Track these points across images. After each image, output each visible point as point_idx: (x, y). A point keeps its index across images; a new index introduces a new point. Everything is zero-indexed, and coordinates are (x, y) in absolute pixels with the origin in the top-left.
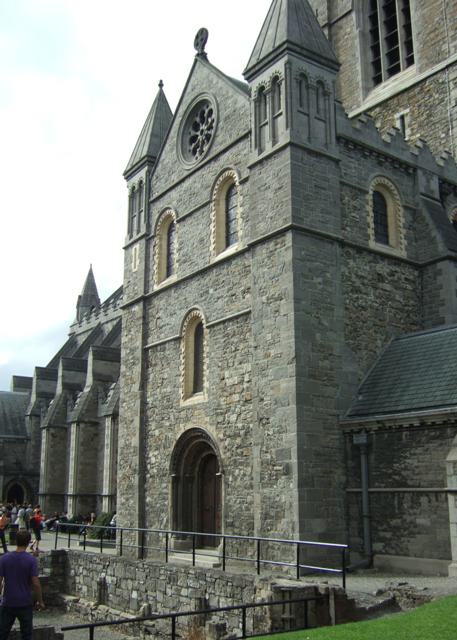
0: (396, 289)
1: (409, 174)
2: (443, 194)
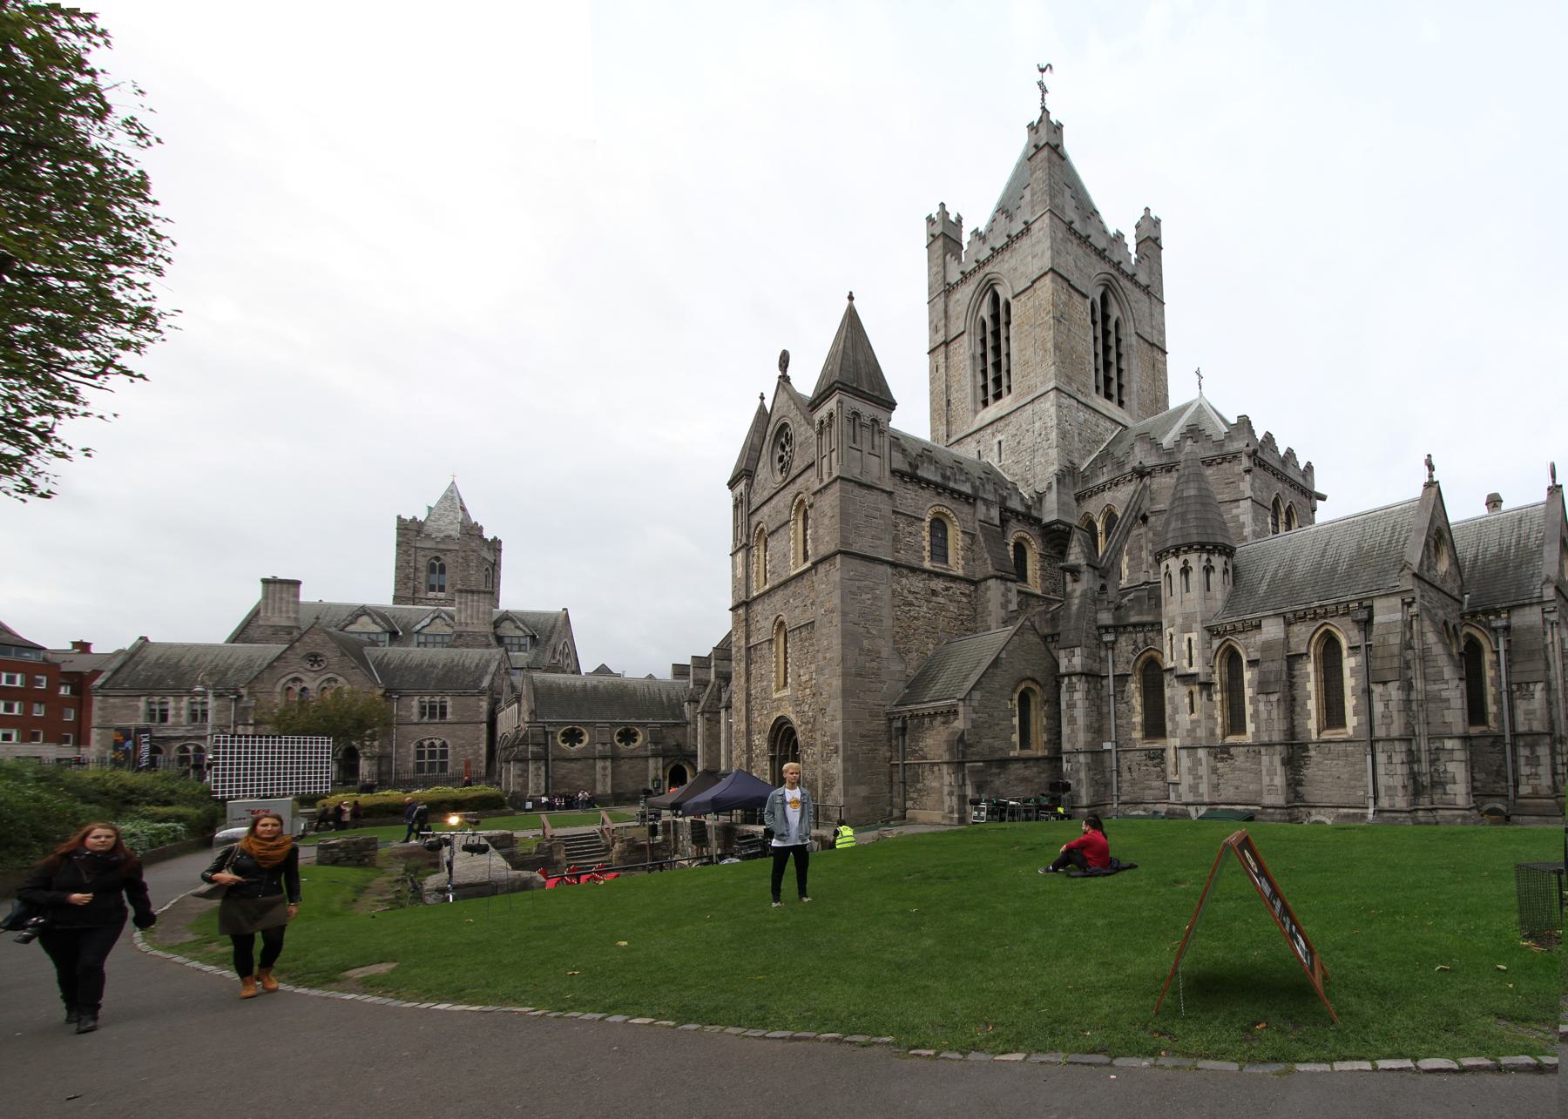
1: (969, 504)
2: (1004, 521)
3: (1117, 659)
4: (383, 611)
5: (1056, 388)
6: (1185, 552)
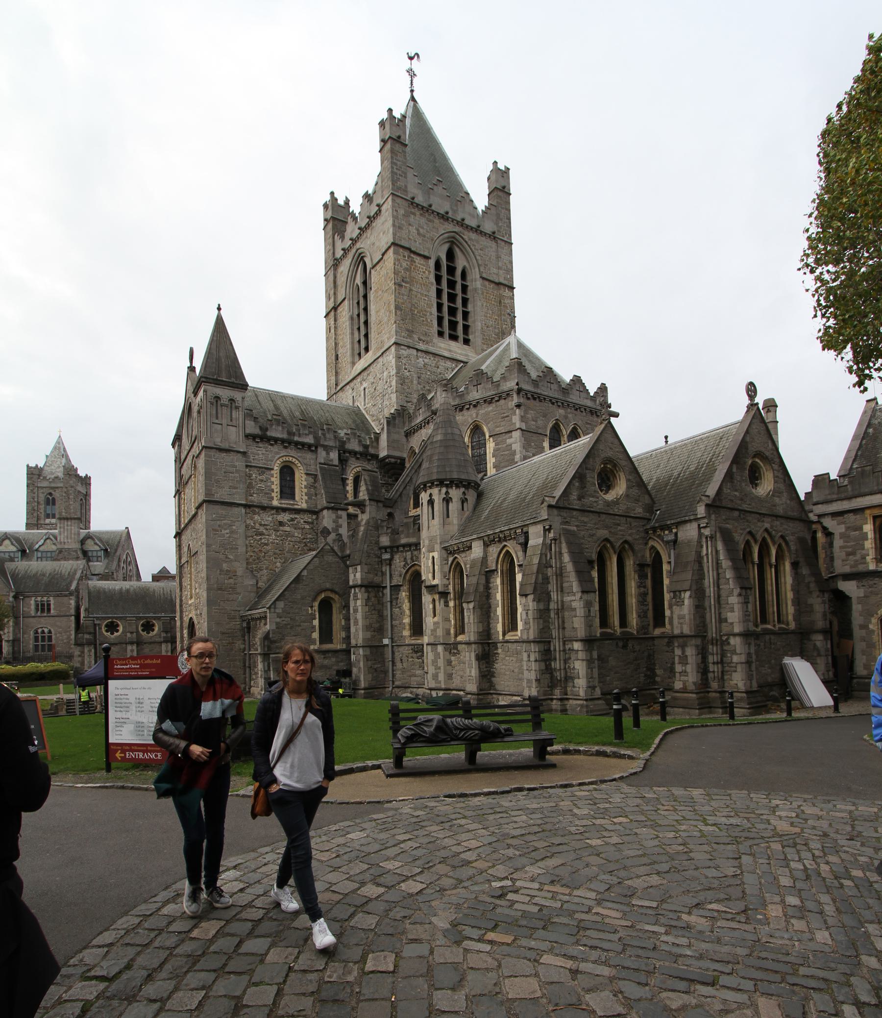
1: (312, 451)
2: (343, 461)
3: (393, 573)
5: (395, 343)
6: (430, 487)
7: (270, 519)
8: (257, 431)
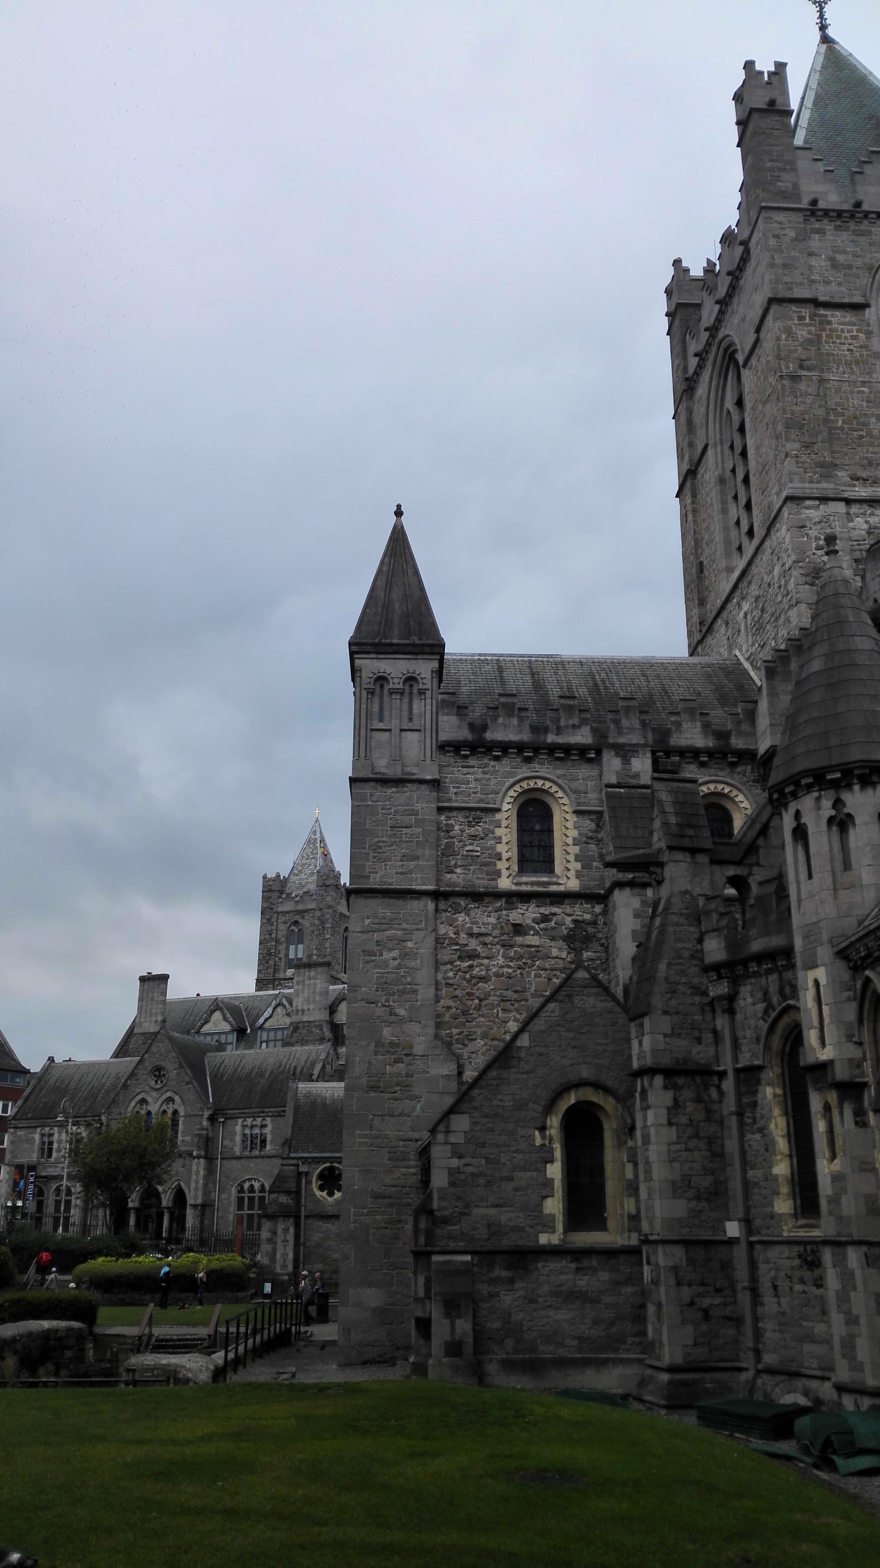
0: (553, 939)
1: (591, 760)
3: (740, 1033)
4: (237, 1003)
6: (795, 795)
7: (492, 920)
8: (464, 734)
